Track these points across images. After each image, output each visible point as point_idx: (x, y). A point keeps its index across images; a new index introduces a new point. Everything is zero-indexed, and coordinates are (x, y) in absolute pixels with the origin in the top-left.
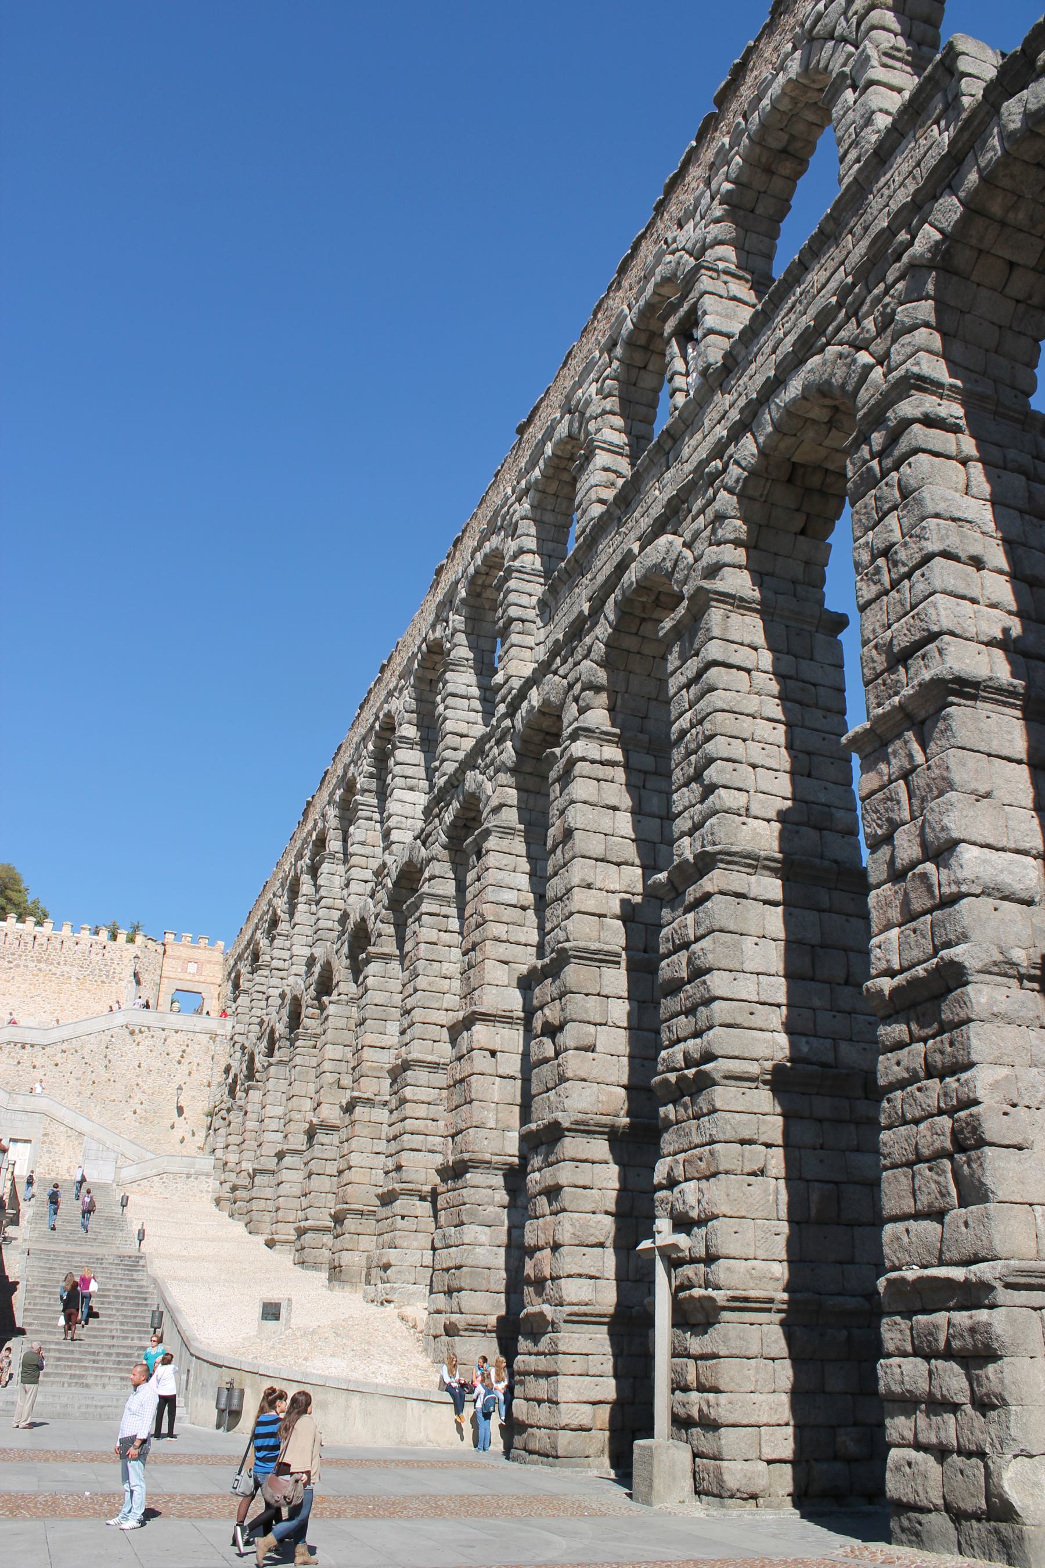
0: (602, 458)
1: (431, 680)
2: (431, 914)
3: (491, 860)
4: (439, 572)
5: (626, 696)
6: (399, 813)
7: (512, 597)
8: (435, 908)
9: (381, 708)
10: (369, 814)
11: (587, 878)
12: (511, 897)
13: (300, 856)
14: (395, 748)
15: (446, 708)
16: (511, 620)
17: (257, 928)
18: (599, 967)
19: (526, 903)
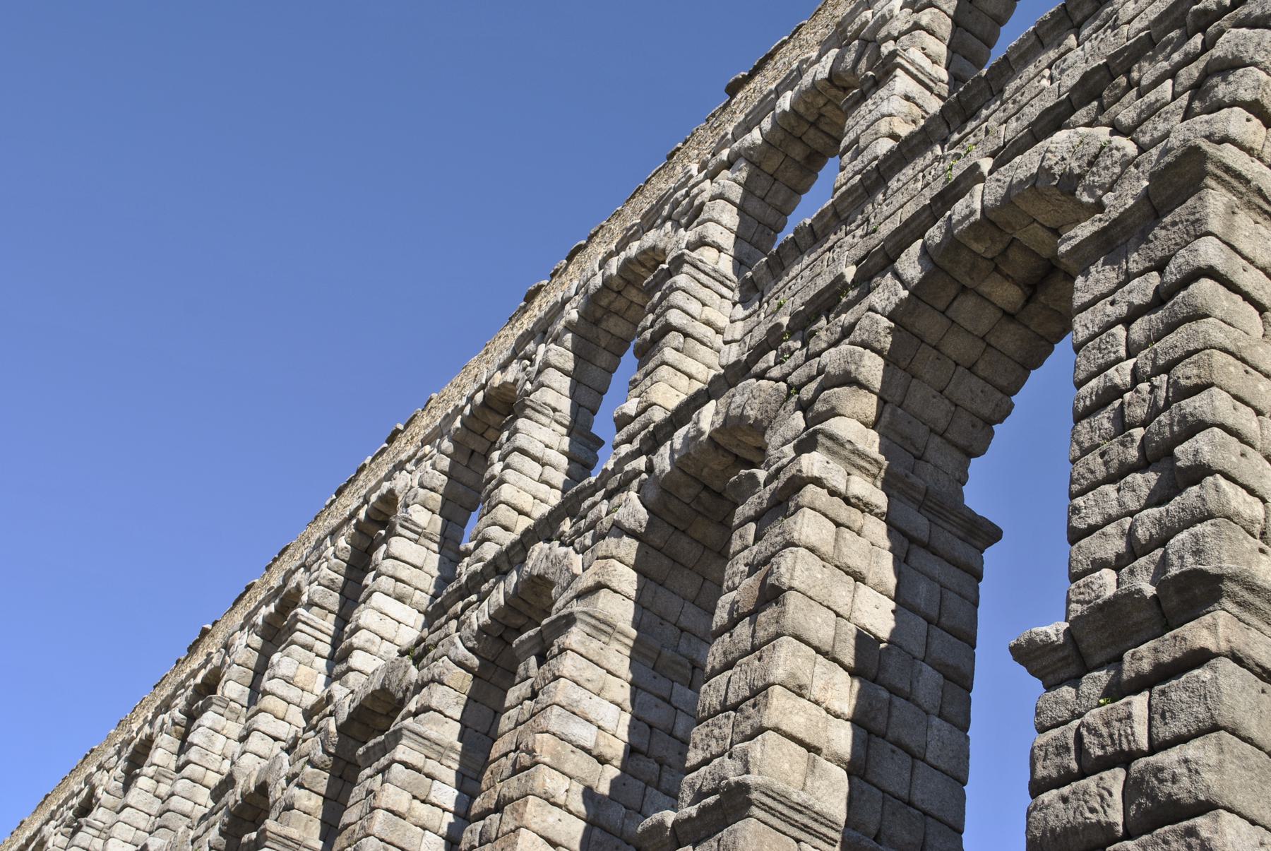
0: (902, 82)
1: (473, 452)
2: (407, 765)
3: (568, 664)
4: (530, 297)
5: (900, 411)
6: (373, 627)
7: (678, 298)
8: (416, 758)
9: (378, 485)
10: (309, 640)
11: (799, 674)
12: (586, 735)
13: (166, 706)
14: (392, 533)
15: (507, 467)
16: (669, 328)
17: (52, 816)
18: (798, 841)
19: (608, 752)
